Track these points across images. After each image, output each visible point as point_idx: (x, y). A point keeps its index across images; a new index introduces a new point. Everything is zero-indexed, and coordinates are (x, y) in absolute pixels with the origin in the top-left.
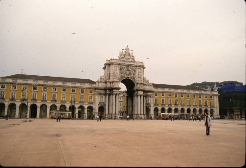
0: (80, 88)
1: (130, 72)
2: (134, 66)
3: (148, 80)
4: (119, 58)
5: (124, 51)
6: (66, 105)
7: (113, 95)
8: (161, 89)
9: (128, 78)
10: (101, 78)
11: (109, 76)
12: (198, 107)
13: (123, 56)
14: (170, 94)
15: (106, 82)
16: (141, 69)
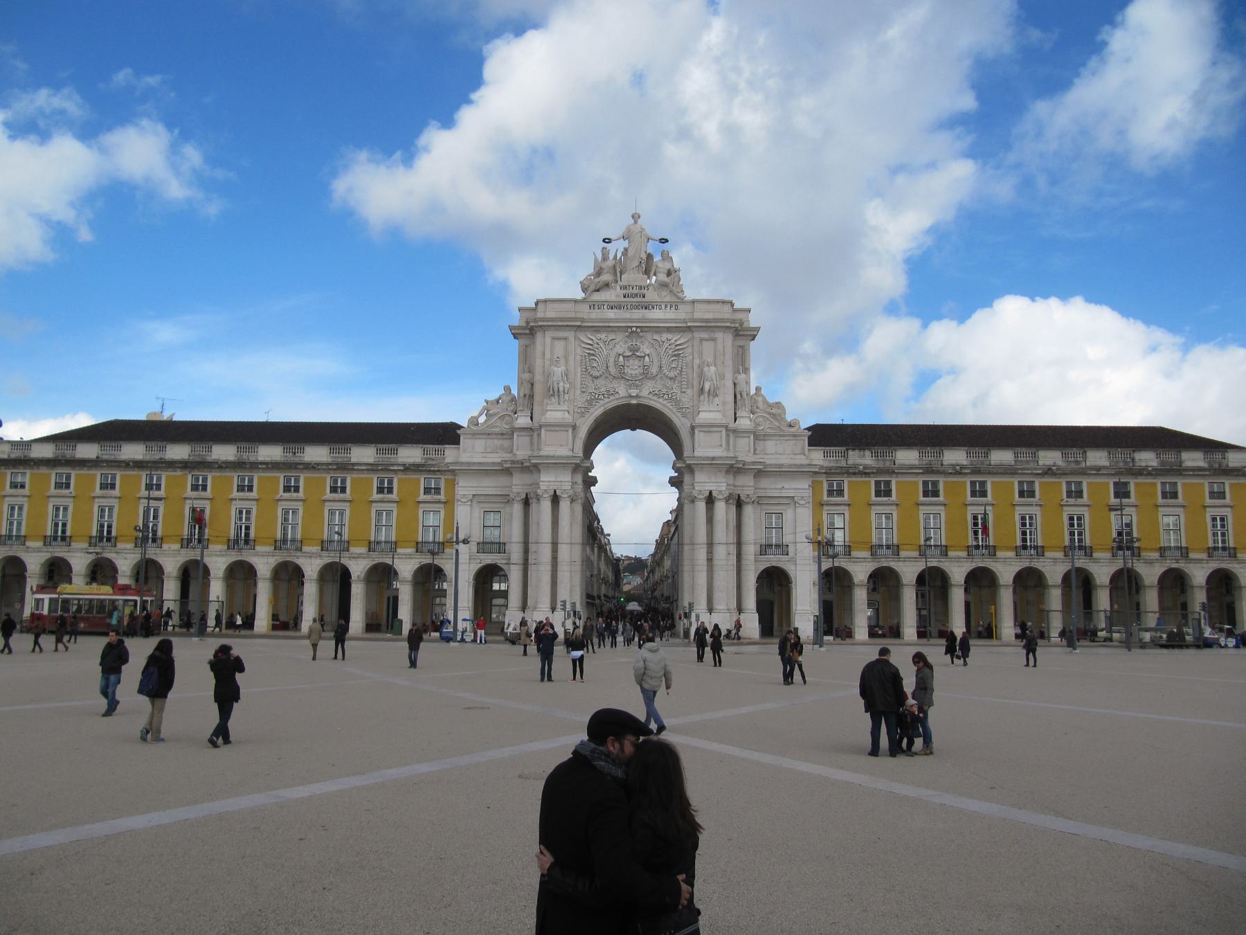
0: (373, 468)
1: (646, 368)
2: (669, 330)
3: (778, 405)
4: (584, 290)
5: (617, 248)
6: (301, 562)
7: (538, 498)
8: (868, 453)
9: (637, 396)
10: (487, 410)
11: (532, 396)
12: (1150, 562)
13: (606, 277)
14: (935, 483)
15: (510, 434)
16: (720, 342)
